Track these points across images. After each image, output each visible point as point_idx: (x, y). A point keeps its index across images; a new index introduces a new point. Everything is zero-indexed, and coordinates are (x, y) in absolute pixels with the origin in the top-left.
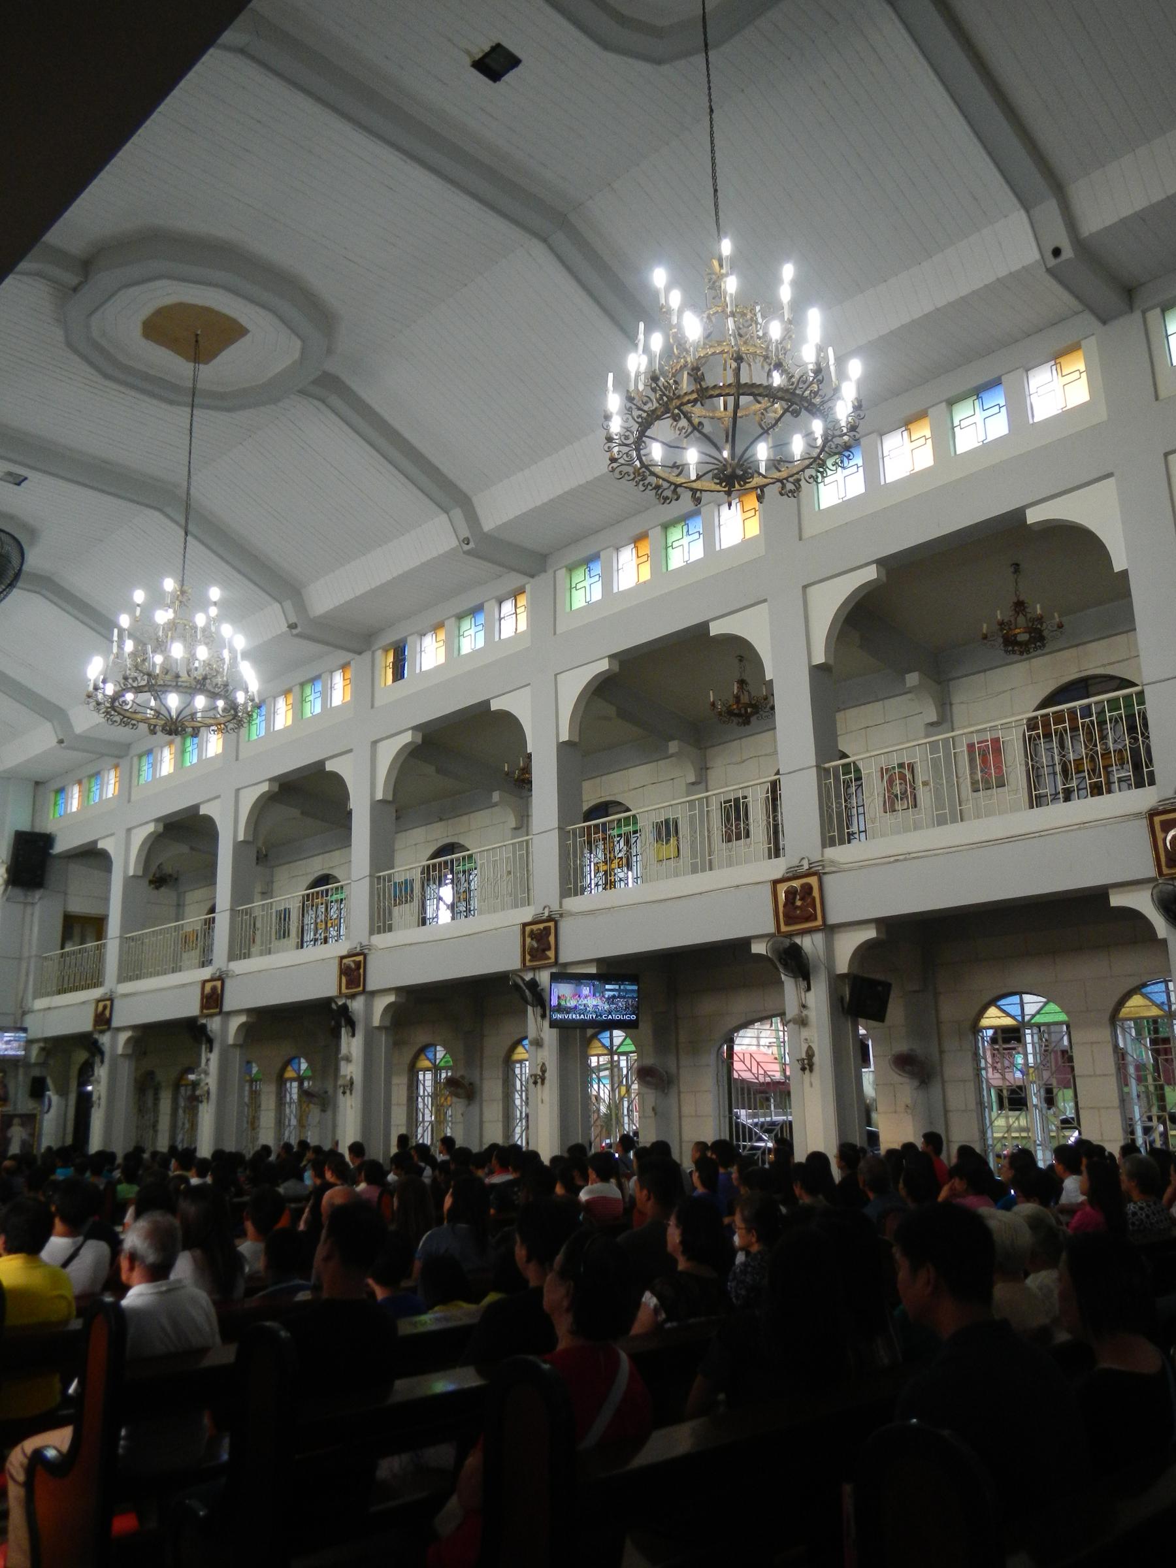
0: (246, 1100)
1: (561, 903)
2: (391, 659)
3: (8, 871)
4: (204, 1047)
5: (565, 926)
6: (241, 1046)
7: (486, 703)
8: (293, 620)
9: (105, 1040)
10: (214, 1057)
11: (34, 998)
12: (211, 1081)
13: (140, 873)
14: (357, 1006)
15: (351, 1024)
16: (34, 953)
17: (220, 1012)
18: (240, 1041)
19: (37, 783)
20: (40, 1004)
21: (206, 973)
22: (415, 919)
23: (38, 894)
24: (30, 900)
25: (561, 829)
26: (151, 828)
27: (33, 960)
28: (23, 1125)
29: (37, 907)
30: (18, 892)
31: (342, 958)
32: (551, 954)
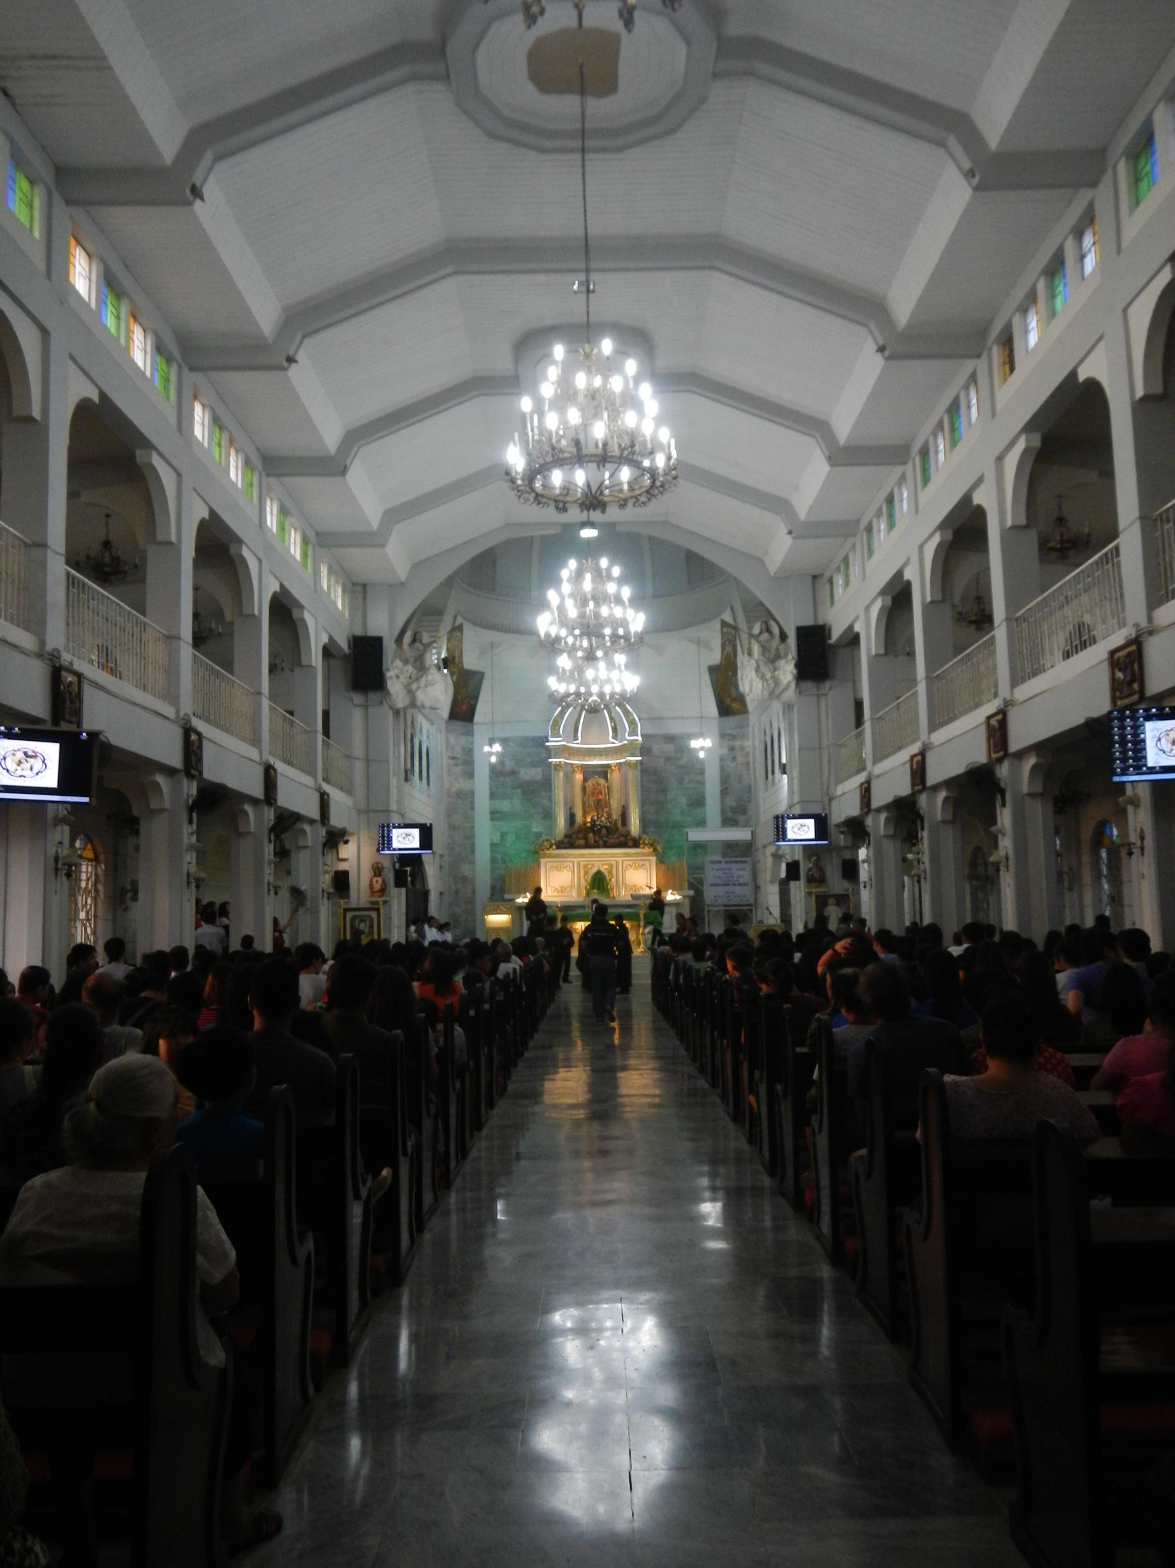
1: (1150, 619)
2: (1007, 352)
3: (797, 666)
5: (1154, 650)
6: (953, 822)
7: (1073, 374)
8: (881, 342)
9: (869, 821)
10: (925, 834)
12: (926, 859)
13: (882, 651)
14: (1003, 771)
15: (1002, 792)
17: (924, 788)
18: (949, 817)
19: (815, 577)
20: (840, 790)
21: (915, 748)
23: (828, 684)
24: (822, 691)
25: (1143, 518)
26: (879, 604)
28: (838, 904)
30: (808, 685)
31: (989, 718)
32: (1136, 686)
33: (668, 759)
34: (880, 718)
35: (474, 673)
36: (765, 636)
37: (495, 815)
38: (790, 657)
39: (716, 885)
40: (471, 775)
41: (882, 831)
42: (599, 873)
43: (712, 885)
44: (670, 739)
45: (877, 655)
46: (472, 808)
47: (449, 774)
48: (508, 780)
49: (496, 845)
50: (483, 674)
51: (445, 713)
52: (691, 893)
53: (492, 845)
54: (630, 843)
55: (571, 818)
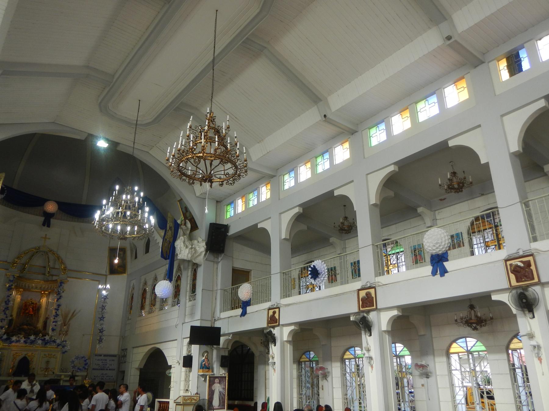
0: (353, 370)
3: (207, 244)
4: (363, 333)
9: (276, 331)
11: (221, 312)
16: (219, 287)
19: (217, 201)
20: (224, 315)
22: (469, 253)
24: (216, 260)
26: (297, 210)
27: (219, 292)
28: (220, 383)
29: (220, 265)
31: (506, 261)
34: (284, 273)
36: (183, 227)
38: (200, 240)
39: (98, 369)
41: (285, 338)
43: (94, 369)
45: (285, 239)
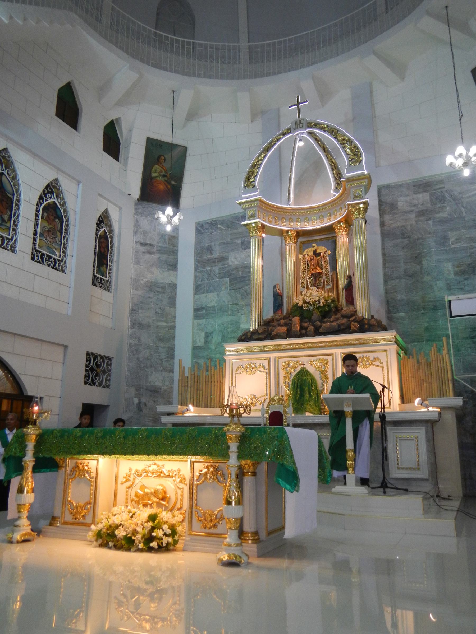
33: (421, 213)
35: (172, 146)
37: (199, 312)
40: (173, 266)
42: (303, 372)
44: (423, 186)
46: (173, 302)
47: (137, 262)
48: (216, 269)
49: (200, 348)
50: (186, 148)
51: (136, 193)
52: (458, 401)
53: (195, 348)
54: (355, 326)
55: (278, 299)
